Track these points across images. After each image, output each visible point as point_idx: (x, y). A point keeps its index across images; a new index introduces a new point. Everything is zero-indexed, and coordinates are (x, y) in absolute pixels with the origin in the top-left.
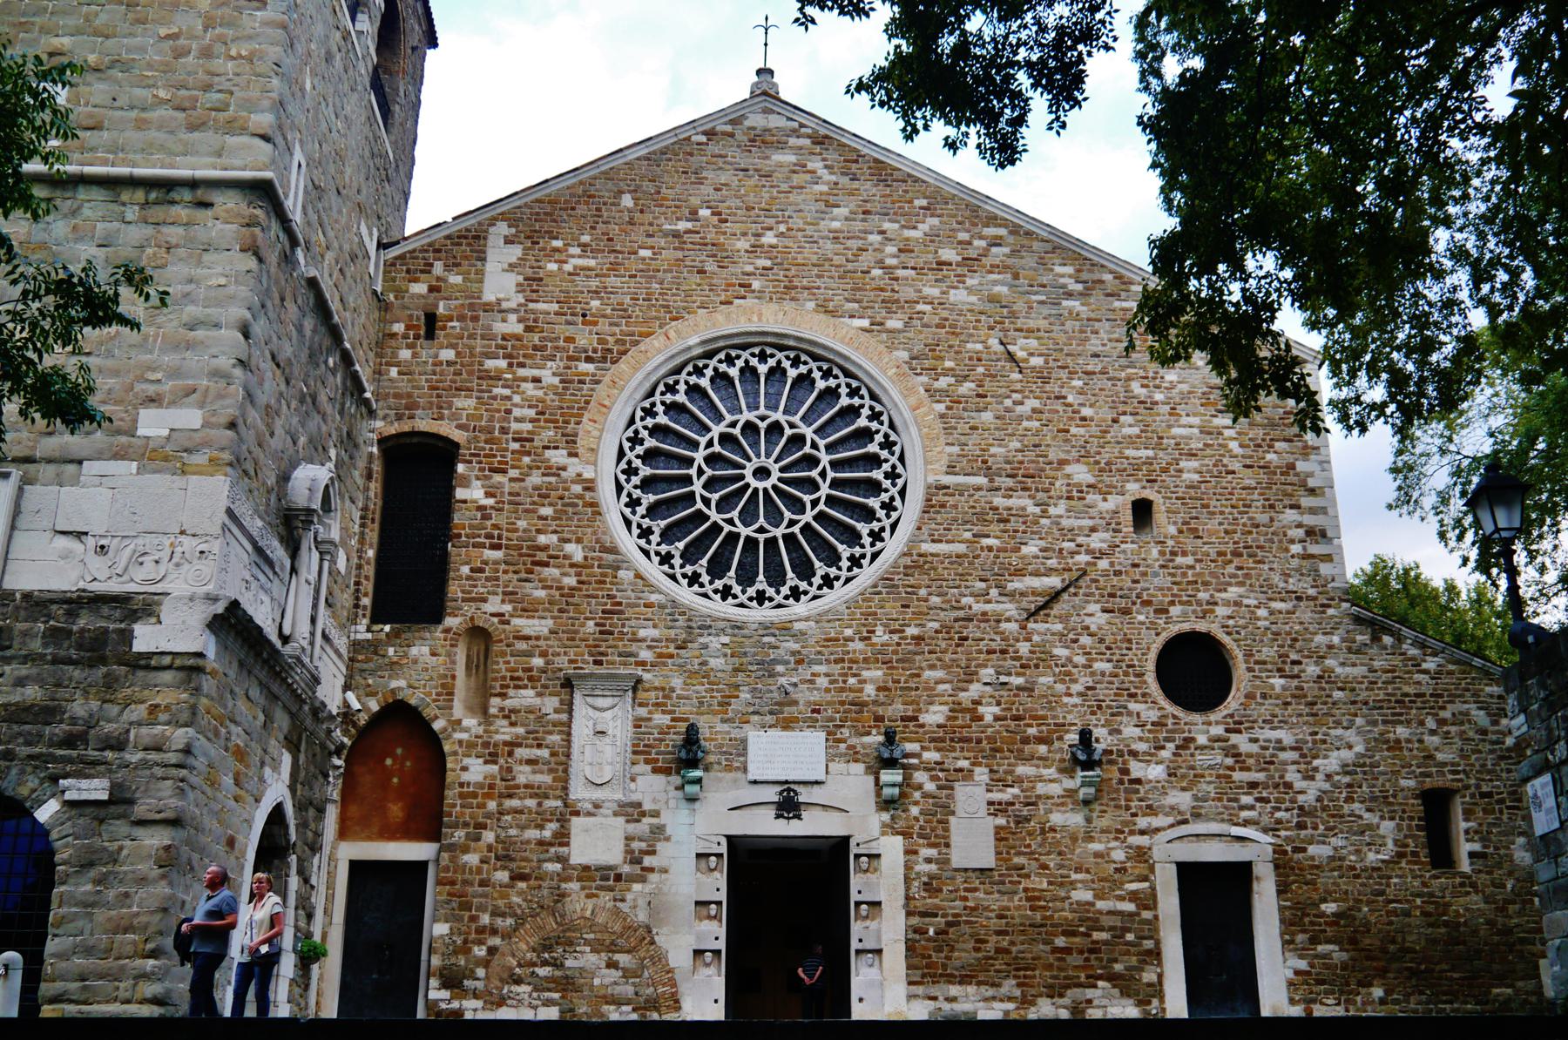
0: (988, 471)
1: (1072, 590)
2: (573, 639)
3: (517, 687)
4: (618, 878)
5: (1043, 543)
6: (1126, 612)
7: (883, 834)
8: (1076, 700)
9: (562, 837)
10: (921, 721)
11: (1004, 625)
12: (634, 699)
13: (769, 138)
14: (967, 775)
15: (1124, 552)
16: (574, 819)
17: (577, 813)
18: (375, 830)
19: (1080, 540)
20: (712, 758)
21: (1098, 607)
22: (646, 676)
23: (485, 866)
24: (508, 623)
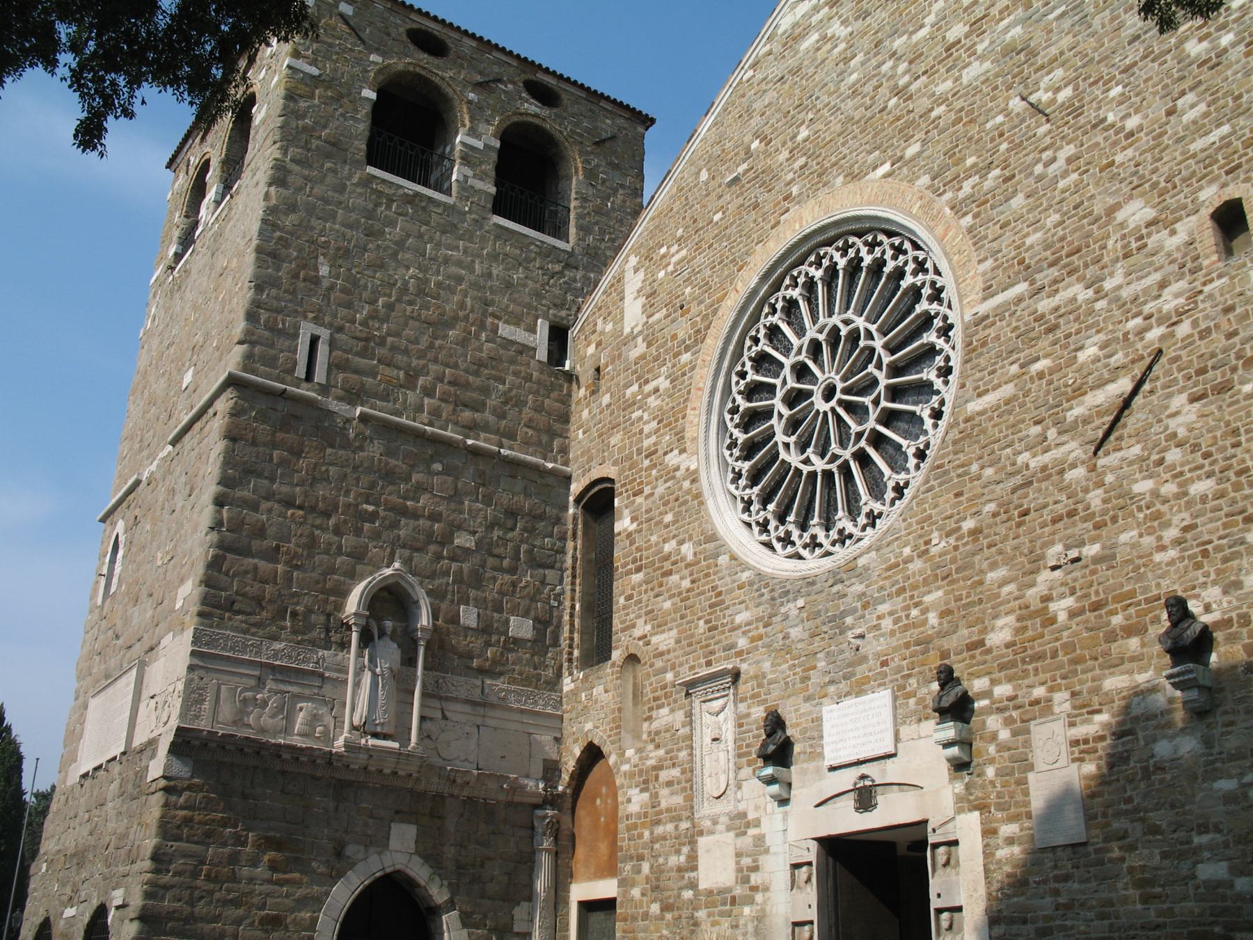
0: (1026, 270)
1: (1147, 387)
2: (690, 645)
3: (659, 707)
4: (733, 900)
5: (1102, 337)
6: (1224, 388)
7: (959, 811)
8: (1172, 553)
9: (692, 863)
10: (988, 643)
11: (1070, 475)
12: (735, 695)
13: (797, 31)
14: (1043, 708)
15: (1210, 296)
16: (702, 841)
17: (701, 833)
18: (592, 870)
19: (1147, 309)
20: (797, 749)
21: (1179, 401)
22: (744, 667)
23: (645, 899)
24: (648, 643)
